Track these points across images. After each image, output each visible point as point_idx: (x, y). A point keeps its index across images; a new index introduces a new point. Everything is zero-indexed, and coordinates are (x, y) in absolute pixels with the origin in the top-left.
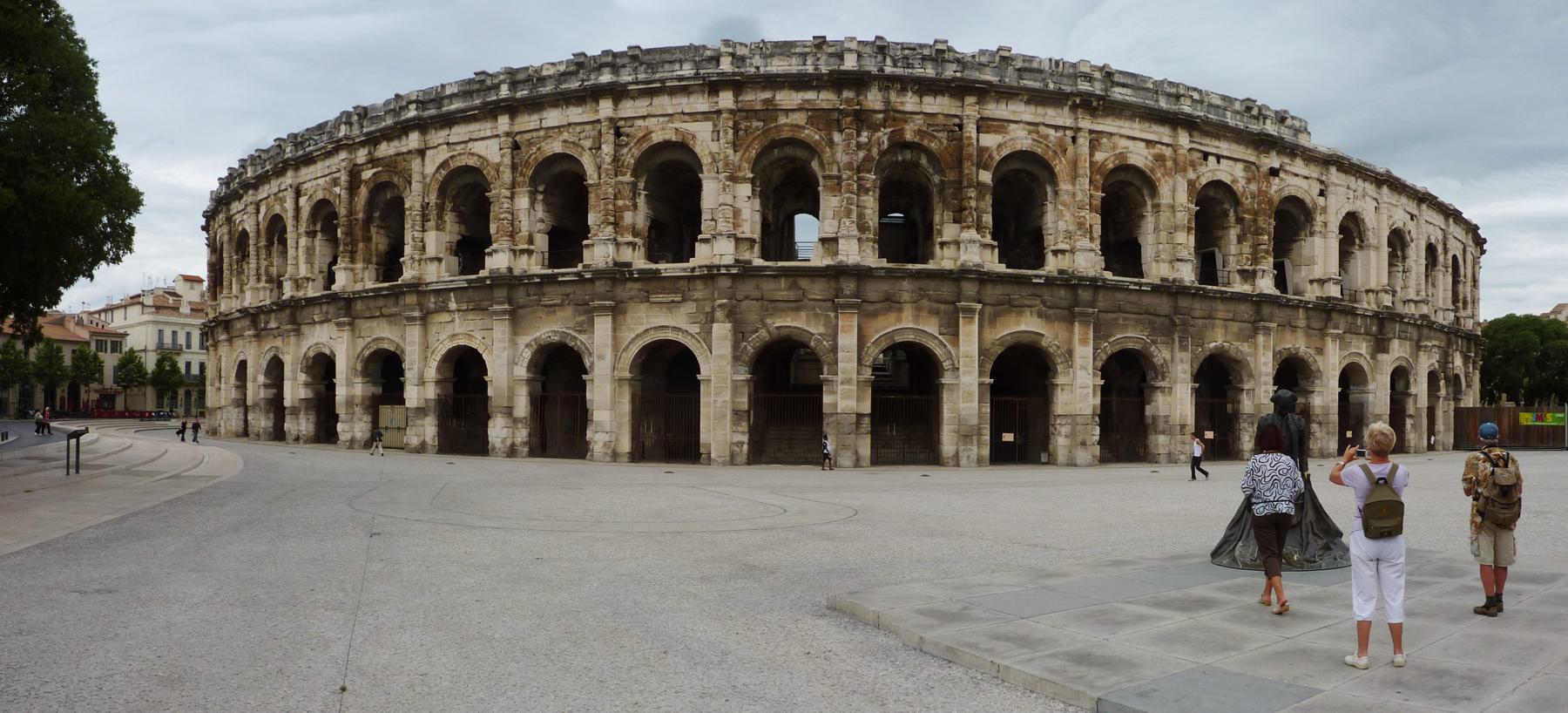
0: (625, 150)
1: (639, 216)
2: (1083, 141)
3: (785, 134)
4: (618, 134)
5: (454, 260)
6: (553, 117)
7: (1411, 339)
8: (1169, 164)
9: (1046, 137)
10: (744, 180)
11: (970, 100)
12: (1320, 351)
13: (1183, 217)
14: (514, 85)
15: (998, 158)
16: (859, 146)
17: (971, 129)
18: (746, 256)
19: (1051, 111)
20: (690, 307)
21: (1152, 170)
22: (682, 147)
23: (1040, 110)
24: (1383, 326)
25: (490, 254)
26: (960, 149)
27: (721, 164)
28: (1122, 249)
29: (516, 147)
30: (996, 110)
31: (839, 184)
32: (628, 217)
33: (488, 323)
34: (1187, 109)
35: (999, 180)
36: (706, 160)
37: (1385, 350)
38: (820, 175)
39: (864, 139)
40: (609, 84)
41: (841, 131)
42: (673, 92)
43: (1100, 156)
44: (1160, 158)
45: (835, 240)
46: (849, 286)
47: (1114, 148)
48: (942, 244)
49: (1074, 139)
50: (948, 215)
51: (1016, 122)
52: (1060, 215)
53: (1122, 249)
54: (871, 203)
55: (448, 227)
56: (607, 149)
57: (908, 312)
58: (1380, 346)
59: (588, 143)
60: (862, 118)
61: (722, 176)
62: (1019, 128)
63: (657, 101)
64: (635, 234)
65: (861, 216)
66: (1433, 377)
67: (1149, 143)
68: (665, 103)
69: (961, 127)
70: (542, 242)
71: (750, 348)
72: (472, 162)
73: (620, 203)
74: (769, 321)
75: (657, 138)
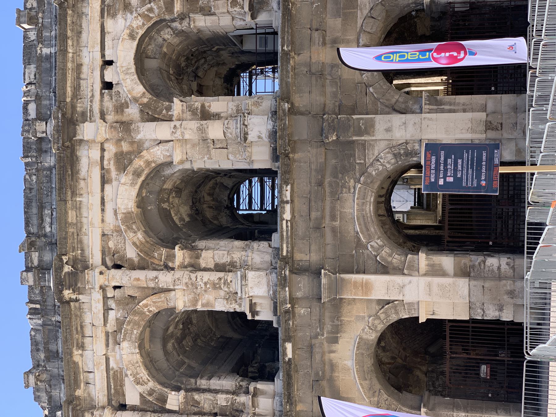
8: (125, 147)
9: (120, 323)
15: (151, 384)
19: (88, 319)
21: (137, 174)
23: (88, 331)
43: (131, 253)
47: (118, 231)
51: (107, 360)
67: (104, 181)
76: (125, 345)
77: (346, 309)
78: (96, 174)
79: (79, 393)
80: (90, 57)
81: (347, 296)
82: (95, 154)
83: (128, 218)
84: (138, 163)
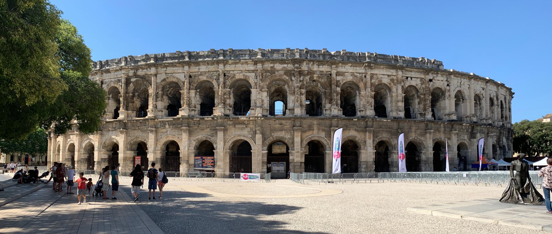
0: (227, 81)
1: (231, 101)
2: (368, 77)
3: (277, 78)
4: (225, 75)
5: (166, 112)
6: (203, 68)
7: (484, 133)
8: (395, 81)
9: (356, 76)
10: (265, 91)
11: (333, 66)
12: (449, 139)
13: (400, 98)
14: (190, 58)
16: (300, 81)
17: (334, 75)
18: (265, 114)
19: (358, 68)
20: (249, 129)
21: (390, 84)
22: (246, 81)
23: (355, 68)
24: (473, 129)
25: (181, 110)
26: (331, 81)
27: (258, 86)
28: (380, 110)
29: (190, 77)
30: (341, 69)
31: (294, 93)
32: (228, 101)
33: (180, 133)
34: (402, 64)
35: (342, 90)
36: (253, 85)
37: (474, 137)
38: (288, 90)
39: (301, 79)
40: (222, 60)
41: (294, 77)
42: (242, 64)
43: (373, 81)
44: (392, 80)
45: (294, 109)
46: (298, 123)
47: (378, 78)
48: (326, 110)
49: (365, 76)
50: (327, 101)
52: (361, 100)
53: (380, 110)
54: (303, 98)
55: (165, 100)
56: (221, 79)
57: (315, 131)
58: (472, 135)
59: (215, 77)
60: (301, 73)
61: (258, 90)
62: (348, 73)
63: (237, 65)
64: (230, 107)
65: (301, 102)
66: (494, 146)
67: (388, 76)
68: (240, 67)
69: (331, 74)
70: (199, 107)
71: (268, 142)
72: (174, 80)
73: (225, 97)
74: (273, 134)
75: (238, 77)
76: (352, 77)
77: (363, 133)
78: (390, 74)
79: (340, 64)
80: (413, 74)
81: (367, 134)
82: (394, 74)
83: (381, 81)
84: (392, 84)
